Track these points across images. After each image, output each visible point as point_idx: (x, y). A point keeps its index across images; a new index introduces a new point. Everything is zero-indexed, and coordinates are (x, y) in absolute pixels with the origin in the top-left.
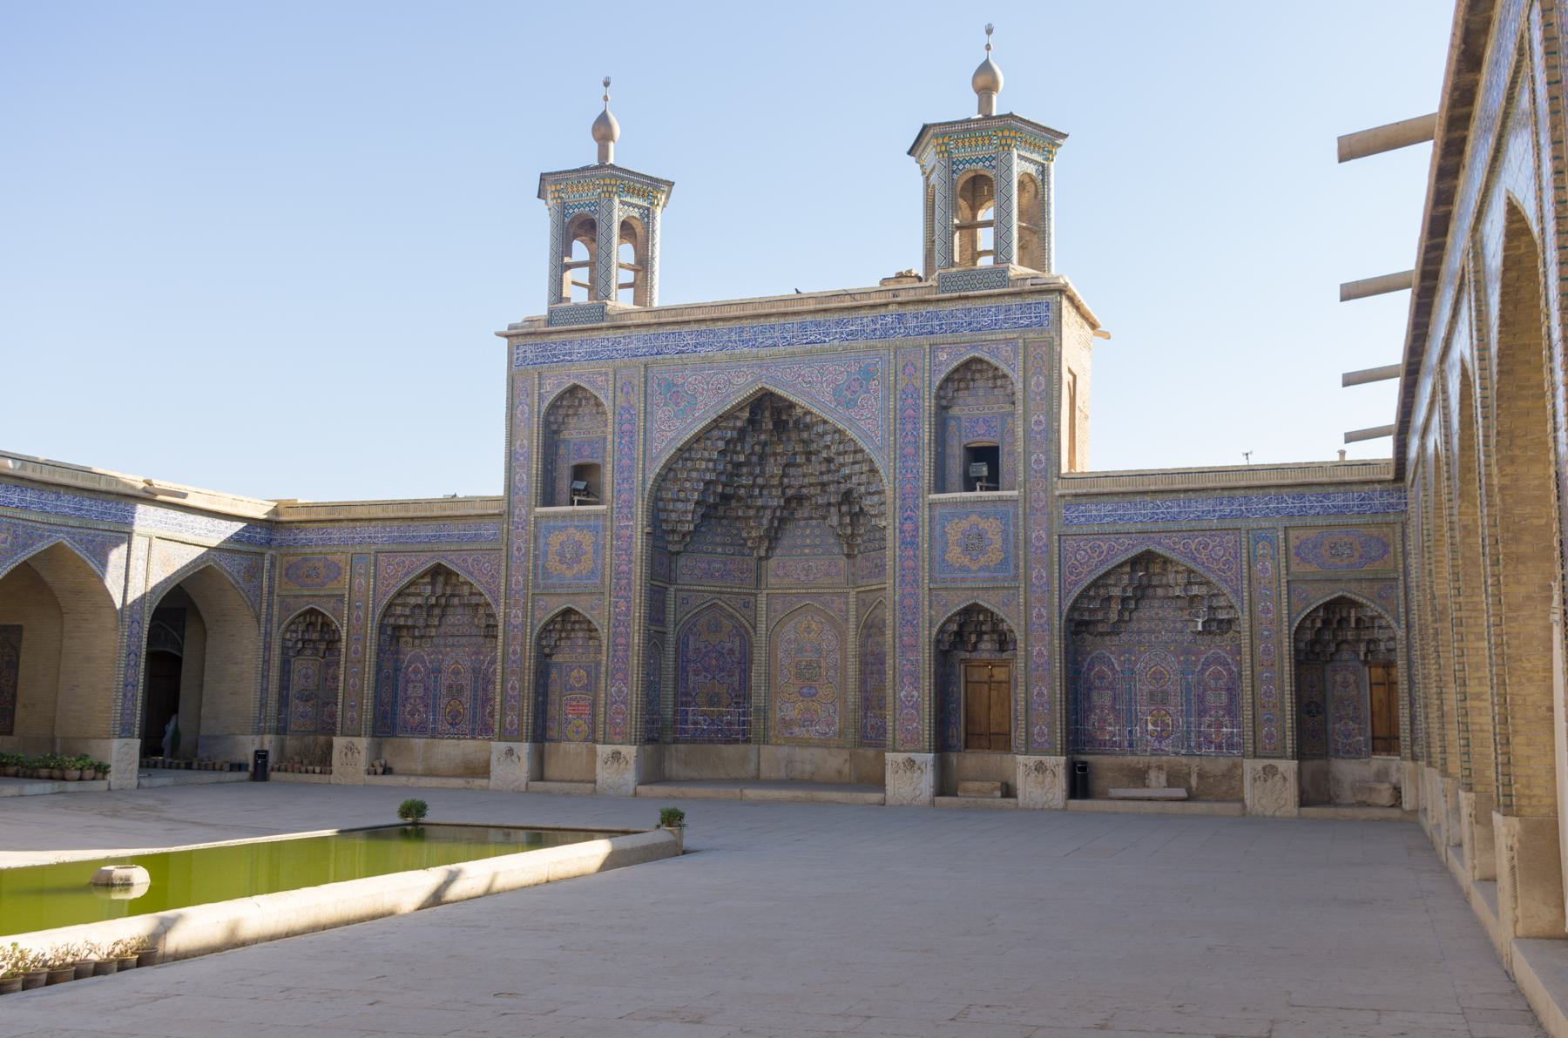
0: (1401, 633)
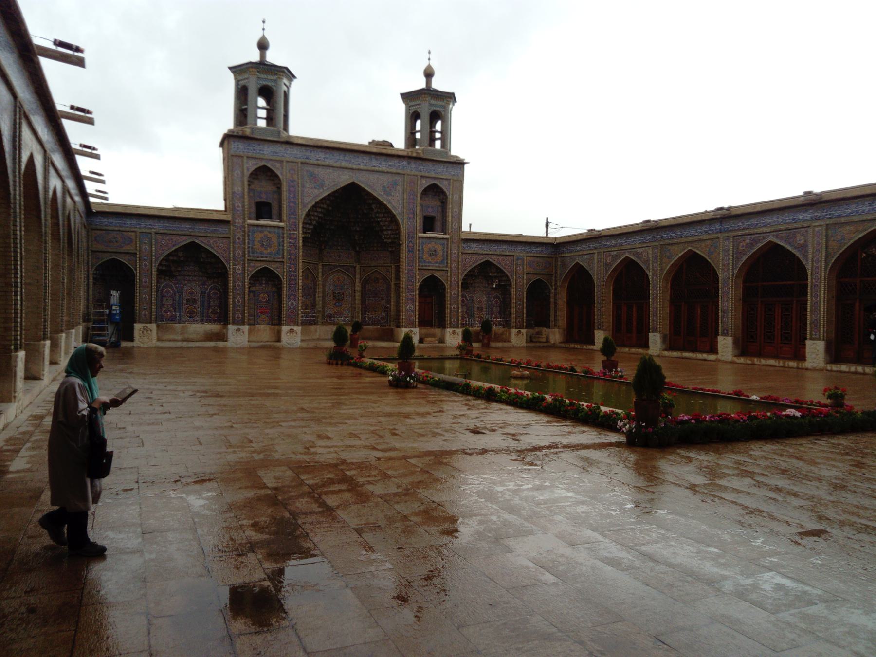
0: (553, 291)
